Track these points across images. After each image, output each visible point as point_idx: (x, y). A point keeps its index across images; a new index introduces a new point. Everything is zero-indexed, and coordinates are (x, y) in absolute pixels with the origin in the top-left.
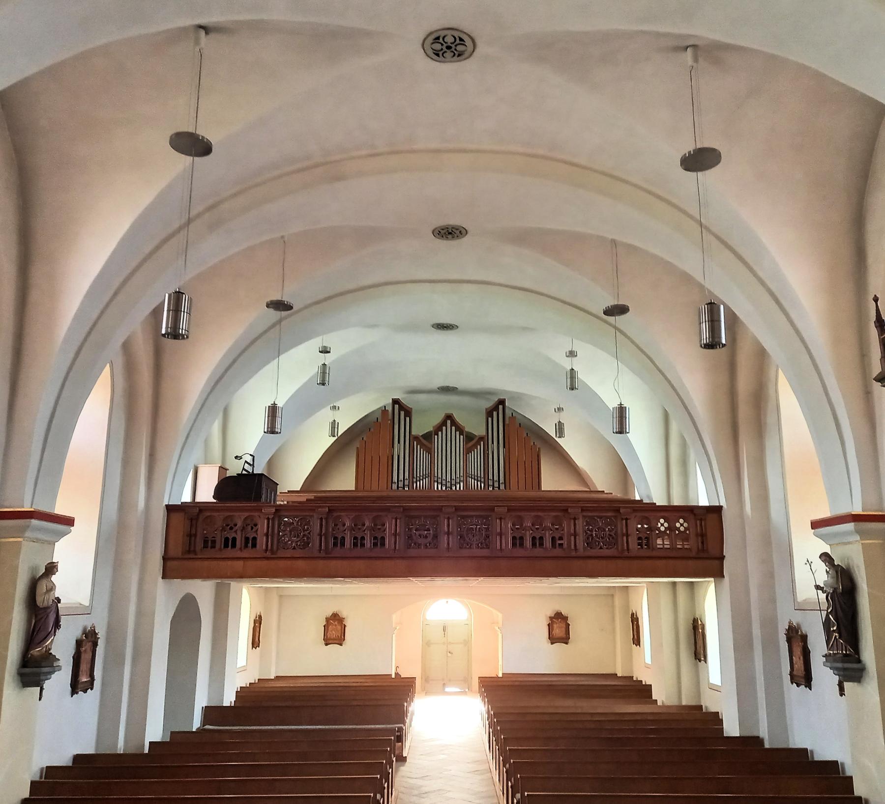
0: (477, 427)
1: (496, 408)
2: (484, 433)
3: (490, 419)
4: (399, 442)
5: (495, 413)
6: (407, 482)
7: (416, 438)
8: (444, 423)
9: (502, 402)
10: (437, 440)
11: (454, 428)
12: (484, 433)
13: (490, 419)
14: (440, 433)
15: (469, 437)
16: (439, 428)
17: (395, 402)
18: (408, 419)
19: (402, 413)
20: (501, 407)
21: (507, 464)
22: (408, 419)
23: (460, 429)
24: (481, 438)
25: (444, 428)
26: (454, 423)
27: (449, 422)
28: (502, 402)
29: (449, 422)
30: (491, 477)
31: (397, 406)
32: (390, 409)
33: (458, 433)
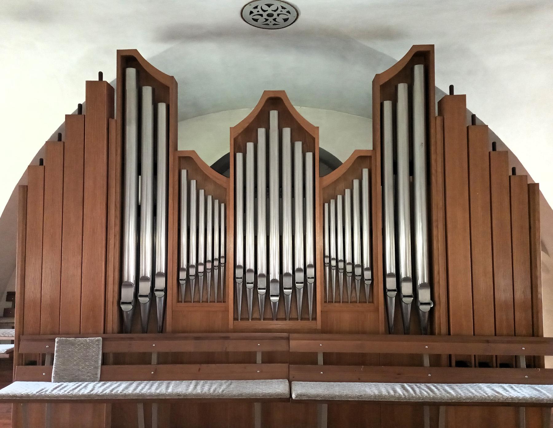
0: (344, 137)
1: (404, 72)
2: (366, 145)
3: (388, 105)
4: (139, 172)
5: (402, 89)
6: (160, 283)
7: (189, 160)
8: (260, 119)
9: (423, 56)
10: (244, 166)
11: (287, 132)
12: (366, 145)
13: (388, 105)
14: (250, 146)
15: (328, 163)
16: (243, 136)
17: (128, 60)
18: (162, 107)
19: (147, 92)
20: (419, 70)
21: (438, 233)
22: (162, 107)
23: (305, 136)
24: (361, 160)
25: (261, 132)
26: (288, 118)
27: (274, 115)
28: (423, 56)
29: (274, 115)
30: (390, 268)
31: (131, 72)
32: (111, 77)
33: (299, 146)
